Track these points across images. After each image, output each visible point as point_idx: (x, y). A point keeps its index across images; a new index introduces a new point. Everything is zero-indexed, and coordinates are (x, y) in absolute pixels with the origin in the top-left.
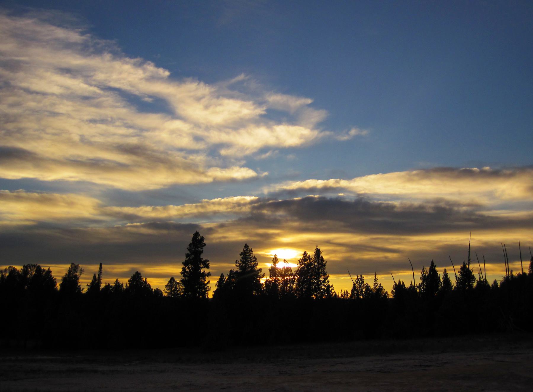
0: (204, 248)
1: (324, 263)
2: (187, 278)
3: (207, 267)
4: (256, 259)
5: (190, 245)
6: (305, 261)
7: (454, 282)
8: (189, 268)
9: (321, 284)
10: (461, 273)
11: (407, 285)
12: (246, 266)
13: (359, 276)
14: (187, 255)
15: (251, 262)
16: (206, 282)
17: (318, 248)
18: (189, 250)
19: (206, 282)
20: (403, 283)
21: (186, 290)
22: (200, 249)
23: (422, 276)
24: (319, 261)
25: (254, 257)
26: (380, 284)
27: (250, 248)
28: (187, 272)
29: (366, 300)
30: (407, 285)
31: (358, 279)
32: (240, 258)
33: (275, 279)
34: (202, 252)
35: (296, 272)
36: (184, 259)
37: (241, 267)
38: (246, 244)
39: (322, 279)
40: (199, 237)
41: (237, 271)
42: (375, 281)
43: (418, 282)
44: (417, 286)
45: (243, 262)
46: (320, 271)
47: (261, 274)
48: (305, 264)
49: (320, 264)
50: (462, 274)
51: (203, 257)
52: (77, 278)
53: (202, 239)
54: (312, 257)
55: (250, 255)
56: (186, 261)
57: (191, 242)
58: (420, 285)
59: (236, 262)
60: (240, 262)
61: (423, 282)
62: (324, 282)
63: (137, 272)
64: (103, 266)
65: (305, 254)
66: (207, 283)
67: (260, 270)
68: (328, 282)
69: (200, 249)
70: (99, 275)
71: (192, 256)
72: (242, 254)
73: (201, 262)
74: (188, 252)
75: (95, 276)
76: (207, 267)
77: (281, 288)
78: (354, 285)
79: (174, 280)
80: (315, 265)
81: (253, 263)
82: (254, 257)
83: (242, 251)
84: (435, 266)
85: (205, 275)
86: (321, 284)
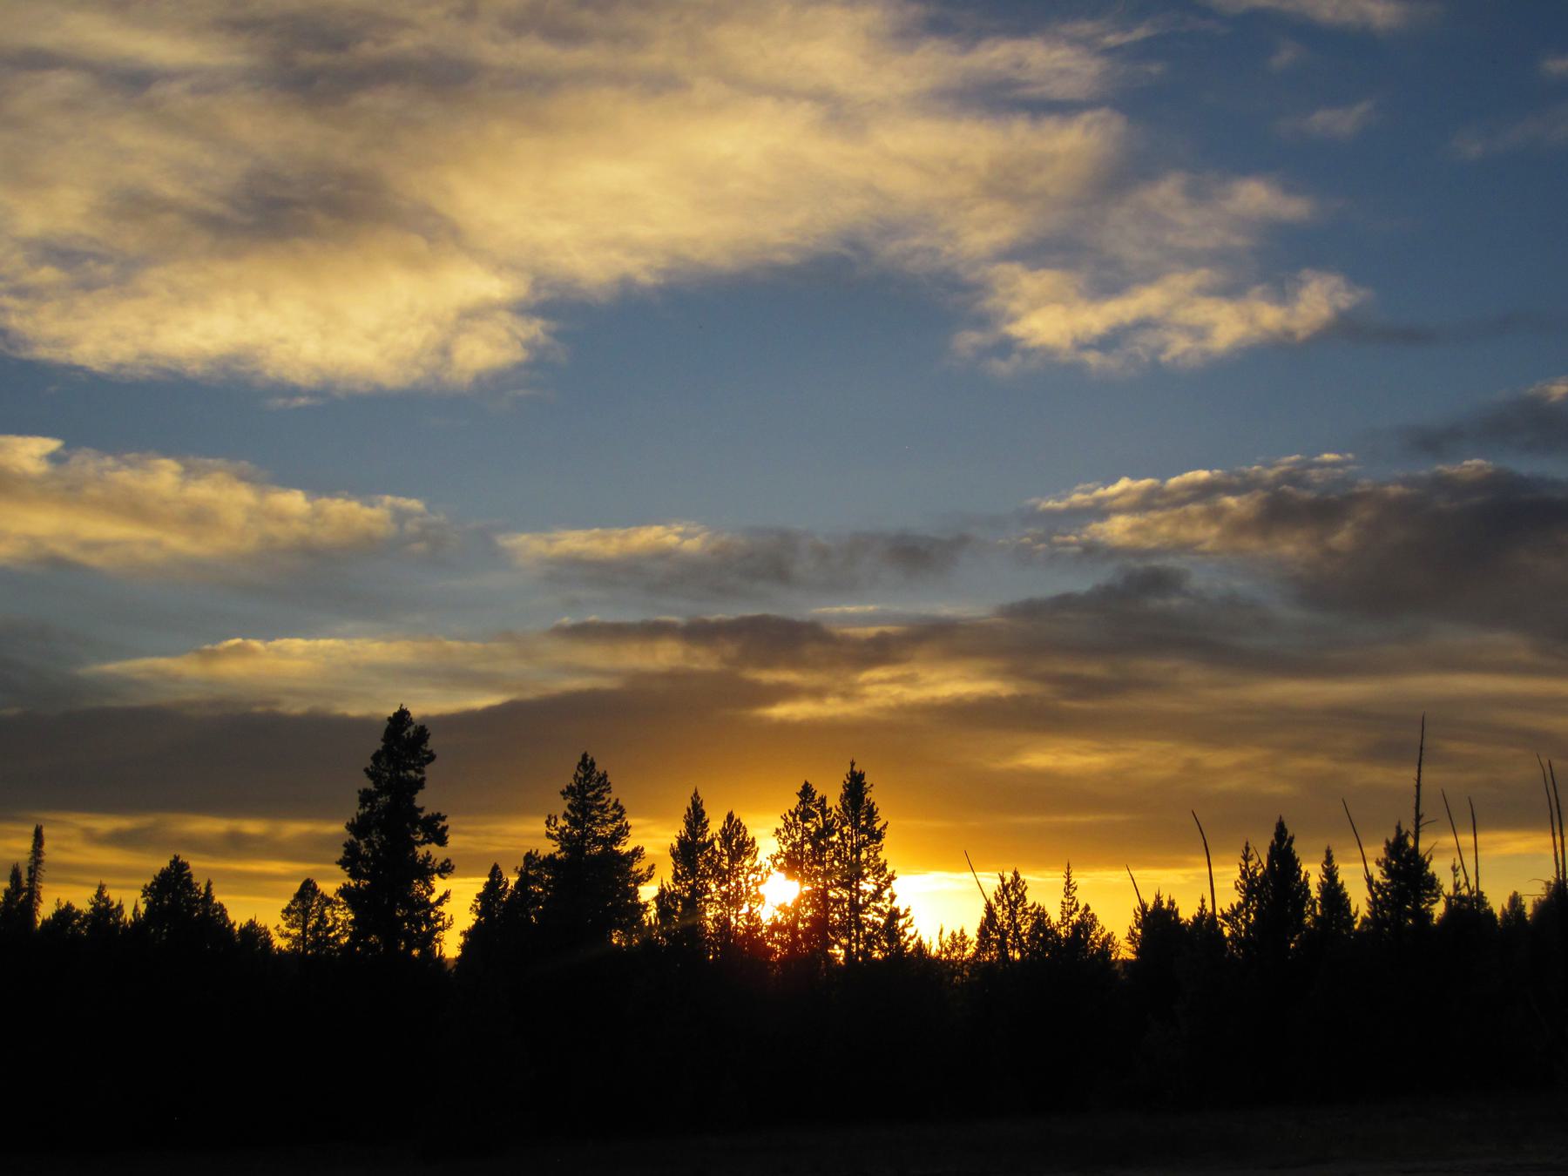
0: (429, 769)
1: (878, 826)
3: (441, 840)
4: (622, 811)
5: (376, 757)
6: (805, 820)
7: (1359, 901)
8: (370, 844)
9: (866, 904)
10: (1388, 867)
11: (1187, 913)
12: (583, 837)
13: (1009, 876)
14: (366, 797)
15: (604, 822)
16: (433, 898)
17: (857, 769)
19: (433, 898)
20: (1172, 903)
21: (361, 927)
22: (412, 773)
23: (1243, 875)
24: (858, 820)
25: (616, 805)
26: (1087, 908)
27: (600, 768)
28: (364, 858)
29: (1038, 969)
30: (1187, 913)
31: (1005, 889)
33: (692, 888)
34: (420, 784)
35: (774, 859)
36: (354, 810)
37: (564, 838)
38: (585, 757)
40: (411, 729)
41: (552, 857)
42: (1068, 894)
43: (1228, 897)
44: (1224, 916)
45: (574, 822)
46: (864, 856)
47: (640, 866)
48: (806, 831)
49: (863, 830)
50: (1390, 872)
51: (426, 802)
54: (834, 802)
55: (597, 797)
56: (362, 818)
57: (380, 745)
58: (1235, 912)
59: (548, 823)
60: (562, 823)
61: (1246, 900)
62: (877, 896)
64: (45, 831)
65: (806, 792)
66: (440, 902)
67: (637, 853)
68: (893, 897)
69: (412, 773)
70: (31, 870)
71: (384, 799)
72: (569, 792)
73: (415, 821)
74: (369, 785)
75: (15, 876)
76: (441, 840)
77: (717, 919)
78: (990, 910)
79: (315, 890)
80: (842, 836)
81: (612, 827)
82: (616, 805)
83: (571, 781)
84: (1291, 840)
85: (432, 872)
86: (866, 904)
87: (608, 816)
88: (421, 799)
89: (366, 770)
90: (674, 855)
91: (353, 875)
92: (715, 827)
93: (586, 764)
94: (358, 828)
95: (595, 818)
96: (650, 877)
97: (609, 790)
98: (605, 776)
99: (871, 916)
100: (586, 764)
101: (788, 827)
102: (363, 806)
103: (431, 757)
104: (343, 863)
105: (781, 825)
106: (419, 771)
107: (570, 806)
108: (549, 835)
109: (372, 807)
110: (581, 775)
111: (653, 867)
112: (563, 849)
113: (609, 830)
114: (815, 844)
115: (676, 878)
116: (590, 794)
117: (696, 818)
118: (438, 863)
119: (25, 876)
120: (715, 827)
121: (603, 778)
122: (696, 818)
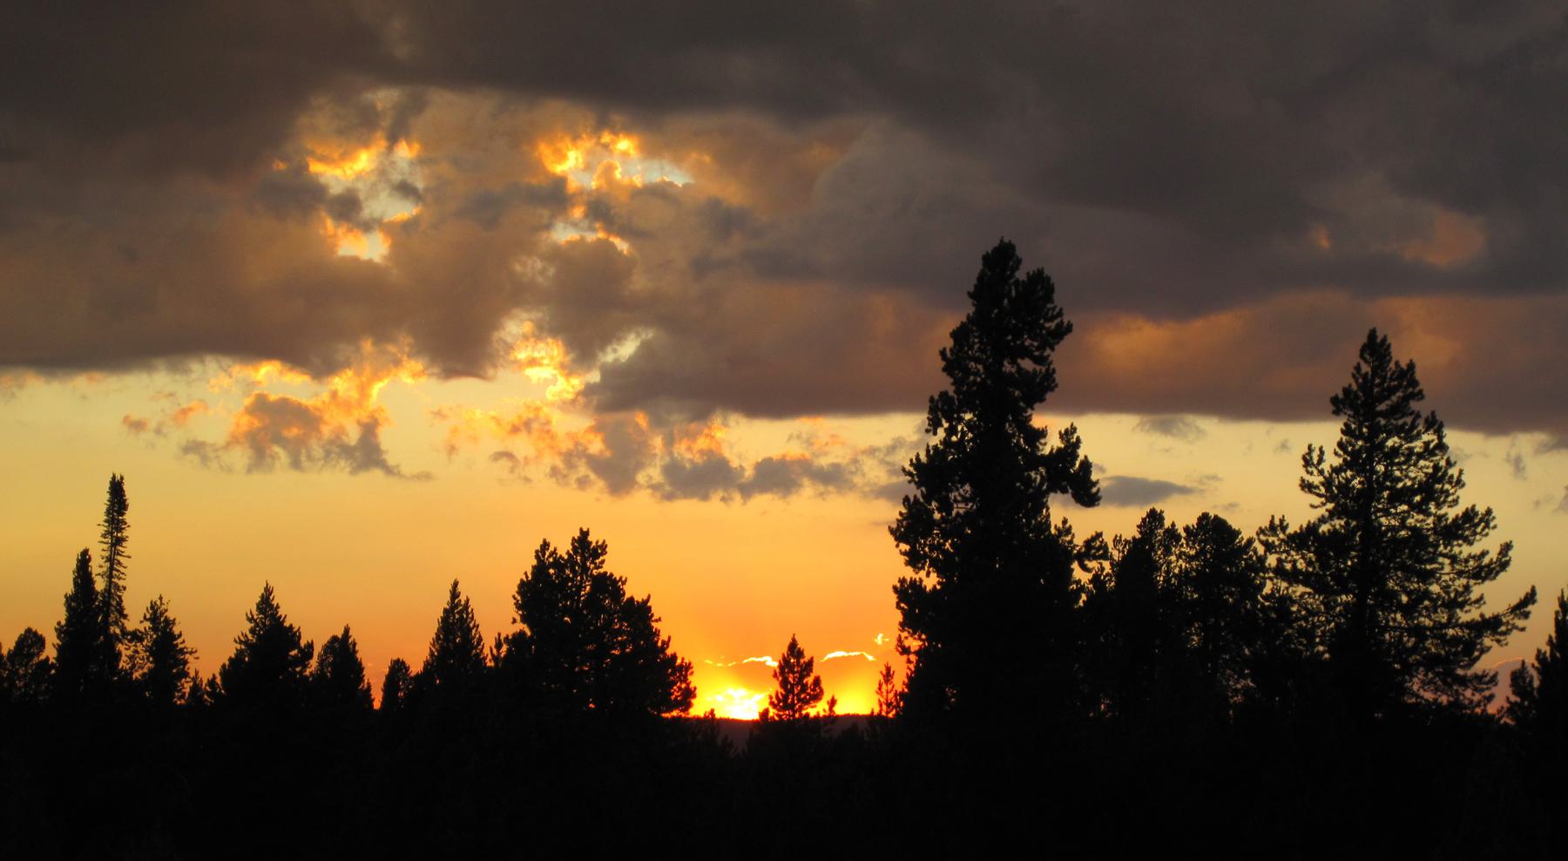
2: (931, 581)
3: (1086, 494)
5: (959, 335)
18: (948, 369)
22: (1027, 364)
27: (1401, 354)
37: (1334, 491)
38: (1372, 335)
41: (1312, 529)
45: (1355, 461)
47: (1487, 545)
53: (1040, 286)
56: (936, 455)
59: (1307, 462)
63: (584, 534)
67: (1474, 522)
69: (1027, 364)
70: (111, 561)
74: (946, 384)
83: (1347, 380)
87: (1418, 446)
89: (943, 353)
91: (914, 559)
95: (1395, 451)
96: (1503, 565)
97: (1420, 395)
98: (1411, 366)
103: (1063, 331)
104: (899, 534)
106: (1040, 360)
107: (1347, 431)
108: (1307, 487)
109: (951, 431)
110: (1365, 368)
111: (1507, 548)
112: (1332, 514)
113: (1417, 473)
116: (1382, 407)
118: (1079, 541)
119: (97, 566)
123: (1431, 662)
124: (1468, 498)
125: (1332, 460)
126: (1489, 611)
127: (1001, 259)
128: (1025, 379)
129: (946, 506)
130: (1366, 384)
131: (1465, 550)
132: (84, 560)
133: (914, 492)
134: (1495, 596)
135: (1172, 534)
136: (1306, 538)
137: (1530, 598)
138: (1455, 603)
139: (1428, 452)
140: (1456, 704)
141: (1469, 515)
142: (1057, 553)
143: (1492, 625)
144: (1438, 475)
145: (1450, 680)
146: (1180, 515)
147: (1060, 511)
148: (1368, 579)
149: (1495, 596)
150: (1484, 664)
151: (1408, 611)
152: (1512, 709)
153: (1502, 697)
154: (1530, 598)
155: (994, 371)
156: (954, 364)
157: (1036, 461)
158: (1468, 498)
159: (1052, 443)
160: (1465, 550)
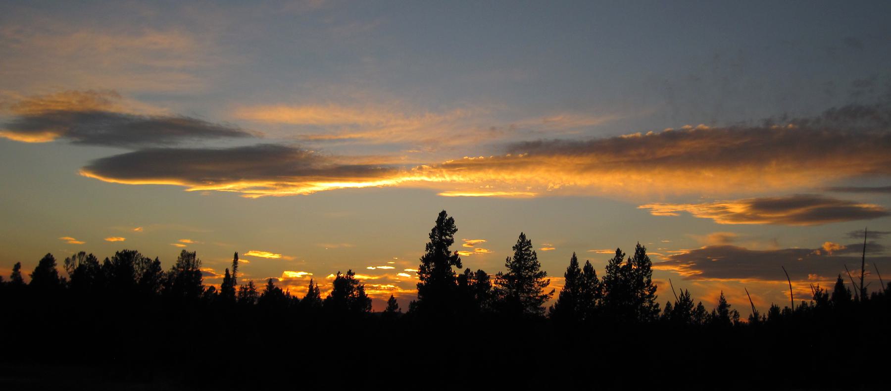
3: (459, 266)
5: (433, 230)
12: (520, 268)
14: (429, 246)
22: (448, 237)
27: (528, 238)
32: (512, 254)
34: (450, 242)
36: (424, 253)
37: (512, 267)
39: (647, 293)
47: (545, 279)
52: (199, 274)
53: (451, 220)
56: (427, 256)
62: (651, 295)
64: (239, 255)
65: (618, 252)
67: (542, 274)
69: (448, 237)
70: (234, 271)
74: (430, 241)
75: (227, 271)
76: (459, 266)
82: (534, 253)
88: (450, 248)
90: (566, 276)
91: (422, 278)
92: (581, 266)
93: (522, 236)
94: (426, 260)
99: (647, 304)
100: (522, 236)
101: (610, 266)
102: (427, 249)
103: (456, 230)
105: (608, 264)
108: (507, 266)
113: (530, 263)
114: (622, 274)
115: (567, 287)
117: (574, 261)
119: (231, 272)
120: (581, 266)
121: (529, 242)
122: (574, 261)
123: (532, 304)
124: (541, 269)
125: (512, 260)
126: (545, 293)
127: (443, 214)
128: (447, 241)
129: (429, 267)
130: (521, 244)
131: (540, 280)
132: (227, 271)
133: (422, 264)
134: (546, 291)
135: (472, 274)
136: (506, 277)
137: (554, 291)
138: (537, 292)
139: (533, 259)
140: (537, 313)
141: (541, 273)
142: (451, 277)
143: (546, 296)
144: (535, 264)
145: (536, 308)
146: (474, 270)
147: (454, 268)
148: (519, 287)
149: (546, 291)
150: (543, 305)
151: (528, 293)
152: (550, 315)
153: (547, 311)
154: (554, 291)
155: (440, 238)
156: (432, 236)
157: (449, 258)
158: (541, 269)
159: (452, 254)
160: (540, 280)
